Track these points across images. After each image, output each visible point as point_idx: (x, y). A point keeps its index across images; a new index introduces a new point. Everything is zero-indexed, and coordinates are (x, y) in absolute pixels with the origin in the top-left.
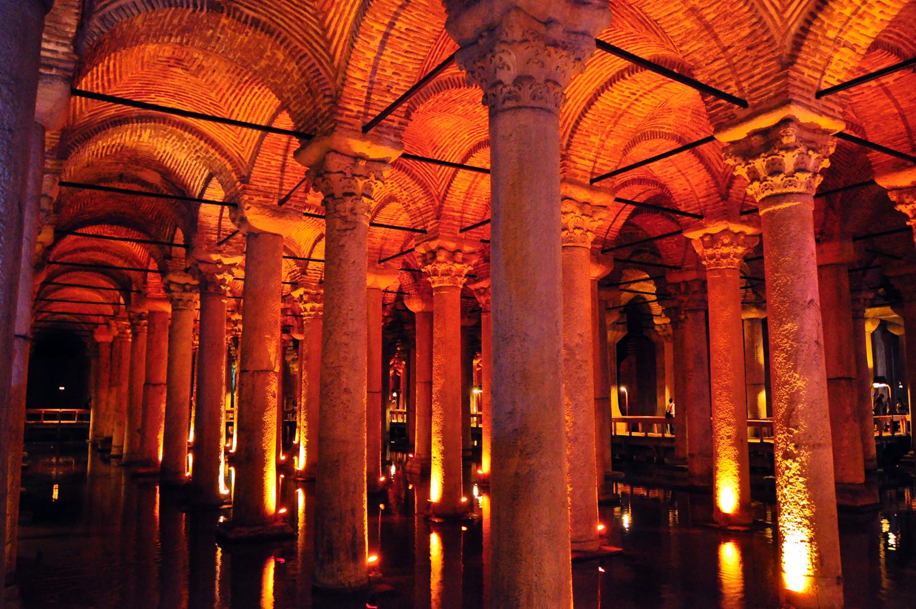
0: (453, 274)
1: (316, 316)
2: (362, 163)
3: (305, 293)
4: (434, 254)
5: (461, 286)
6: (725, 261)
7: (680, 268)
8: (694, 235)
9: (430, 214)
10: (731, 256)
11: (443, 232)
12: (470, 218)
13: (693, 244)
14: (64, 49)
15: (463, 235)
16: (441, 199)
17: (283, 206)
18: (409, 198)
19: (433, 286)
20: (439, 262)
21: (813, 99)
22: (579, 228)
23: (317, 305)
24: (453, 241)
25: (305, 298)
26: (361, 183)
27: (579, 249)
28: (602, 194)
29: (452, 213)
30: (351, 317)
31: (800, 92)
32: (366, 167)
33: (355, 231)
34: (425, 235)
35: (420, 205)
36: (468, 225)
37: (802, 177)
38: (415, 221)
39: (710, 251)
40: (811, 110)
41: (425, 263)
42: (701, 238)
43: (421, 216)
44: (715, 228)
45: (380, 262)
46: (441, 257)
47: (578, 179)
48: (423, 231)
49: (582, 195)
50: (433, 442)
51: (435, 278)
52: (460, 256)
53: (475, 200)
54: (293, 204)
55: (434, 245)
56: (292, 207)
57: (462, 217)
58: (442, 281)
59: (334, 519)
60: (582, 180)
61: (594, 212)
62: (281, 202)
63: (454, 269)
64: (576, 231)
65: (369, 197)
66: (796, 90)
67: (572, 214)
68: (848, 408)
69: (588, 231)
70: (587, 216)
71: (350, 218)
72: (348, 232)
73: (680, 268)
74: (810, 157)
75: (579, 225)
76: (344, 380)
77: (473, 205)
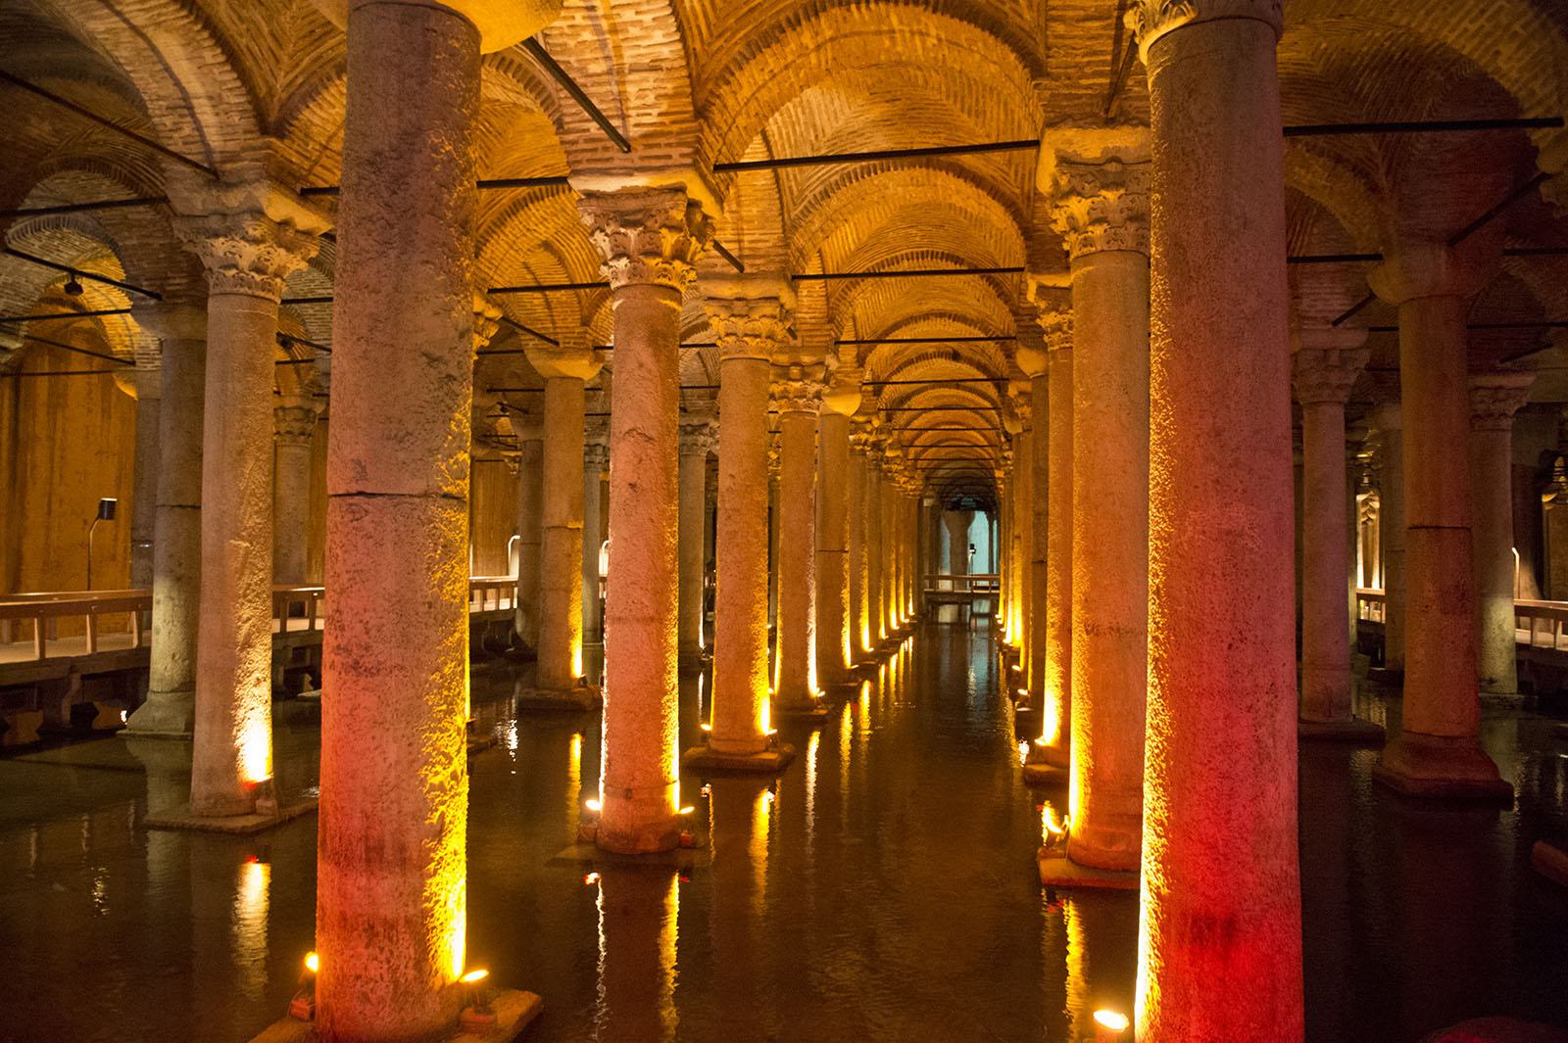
10: (1065, 328)
14: (184, 281)
21: (621, 155)
22: (727, 335)
28: (759, 282)
31: (588, 155)
37: (624, 261)
40: (612, 175)
47: (717, 270)
49: (727, 290)
52: (795, 371)
63: (788, 387)
67: (717, 319)
68: (1429, 586)
69: (746, 335)
74: (625, 235)
75: (730, 331)
77: (805, 299)
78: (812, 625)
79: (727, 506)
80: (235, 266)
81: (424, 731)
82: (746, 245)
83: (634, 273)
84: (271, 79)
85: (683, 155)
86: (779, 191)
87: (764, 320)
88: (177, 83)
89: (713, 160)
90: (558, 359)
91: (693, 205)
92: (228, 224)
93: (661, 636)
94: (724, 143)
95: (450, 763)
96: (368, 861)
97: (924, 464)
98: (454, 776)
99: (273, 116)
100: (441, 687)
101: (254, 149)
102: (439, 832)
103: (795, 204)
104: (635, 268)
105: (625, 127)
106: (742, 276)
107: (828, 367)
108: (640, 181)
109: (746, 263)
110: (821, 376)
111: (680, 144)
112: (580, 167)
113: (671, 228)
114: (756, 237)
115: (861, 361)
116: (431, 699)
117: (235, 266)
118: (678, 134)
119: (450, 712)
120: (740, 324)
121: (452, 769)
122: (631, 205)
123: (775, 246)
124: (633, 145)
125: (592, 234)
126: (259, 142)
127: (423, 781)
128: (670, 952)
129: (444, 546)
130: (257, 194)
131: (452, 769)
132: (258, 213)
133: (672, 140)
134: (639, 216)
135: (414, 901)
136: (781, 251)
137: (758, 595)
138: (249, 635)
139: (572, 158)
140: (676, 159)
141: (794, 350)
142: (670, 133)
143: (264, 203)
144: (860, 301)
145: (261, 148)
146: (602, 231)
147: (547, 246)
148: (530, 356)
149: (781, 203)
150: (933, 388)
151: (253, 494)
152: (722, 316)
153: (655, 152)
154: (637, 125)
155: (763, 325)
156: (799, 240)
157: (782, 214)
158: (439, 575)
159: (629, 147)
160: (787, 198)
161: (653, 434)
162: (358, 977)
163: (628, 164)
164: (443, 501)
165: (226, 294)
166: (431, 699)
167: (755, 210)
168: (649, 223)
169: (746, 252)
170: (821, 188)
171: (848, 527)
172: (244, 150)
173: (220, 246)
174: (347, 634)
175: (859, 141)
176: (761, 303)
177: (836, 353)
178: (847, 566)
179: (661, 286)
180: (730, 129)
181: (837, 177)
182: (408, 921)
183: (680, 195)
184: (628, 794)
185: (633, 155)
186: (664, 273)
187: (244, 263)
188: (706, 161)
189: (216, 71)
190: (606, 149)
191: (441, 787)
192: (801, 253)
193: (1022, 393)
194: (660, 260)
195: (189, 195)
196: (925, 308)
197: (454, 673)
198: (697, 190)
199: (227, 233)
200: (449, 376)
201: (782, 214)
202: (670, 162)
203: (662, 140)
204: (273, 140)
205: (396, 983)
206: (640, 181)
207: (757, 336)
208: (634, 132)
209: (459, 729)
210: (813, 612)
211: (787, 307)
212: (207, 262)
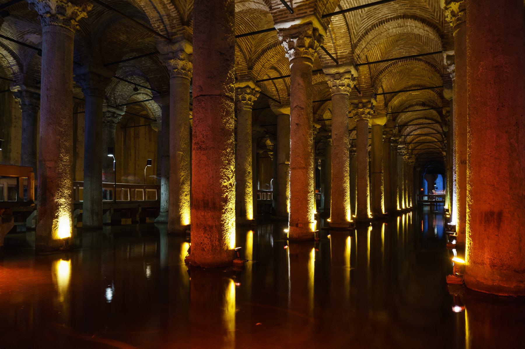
2: (239, 90)
21: (290, 15)
22: (333, 86)
26: (240, 97)
31: (280, 17)
32: (241, 91)
37: (292, 51)
47: (329, 64)
49: (333, 71)
52: (360, 105)
60: (332, 64)
61: (341, 77)
65: (244, 100)
66: (277, 17)
69: (340, 86)
74: (293, 41)
78: (368, 193)
79: (335, 144)
80: (177, 68)
81: (221, 168)
82: (339, 54)
83: (296, 54)
84: (184, 7)
85: (311, 11)
86: (349, 33)
87: (346, 80)
88: (158, 12)
89: (321, 14)
91: (315, 30)
92: (175, 55)
93: (307, 173)
94: (325, 8)
95: (229, 180)
96: (204, 207)
97: (415, 152)
98: (230, 184)
99: (186, 19)
100: (226, 155)
101: (180, 30)
102: (226, 201)
103: (355, 38)
104: (296, 52)
105: (291, 4)
106: (338, 66)
107: (372, 104)
108: (297, 22)
109: (339, 60)
110: (370, 106)
111: (309, 8)
112: (278, 21)
113: (308, 37)
114: (342, 51)
115: (386, 105)
116: (223, 158)
117: (177, 68)
118: (309, 4)
119: (229, 164)
120: (338, 82)
121: (230, 182)
122: (294, 31)
123: (349, 53)
124: (294, 10)
125: (282, 43)
126: (181, 28)
127: (221, 184)
128: (289, 210)
129: (226, 112)
130: (182, 45)
131: (230, 182)
132: (182, 50)
133: (307, 7)
134: (297, 35)
135: (218, 221)
136: (351, 55)
137: (346, 174)
138: (183, 180)
139: (275, 18)
140: (309, 13)
141: (360, 98)
142: (306, 4)
143: (184, 47)
144: (384, 80)
145: (182, 30)
146: (285, 41)
147: (273, 68)
148: (272, 108)
149: (350, 38)
150: (416, 119)
151: (184, 138)
152: (332, 80)
153: (302, 12)
154: (295, 3)
155: (346, 82)
156: (357, 51)
157: (351, 42)
158: (225, 120)
159: (293, 11)
160: (353, 36)
161: (303, 106)
162: (201, 243)
163: (293, 17)
164: (225, 98)
165: (174, 77)
166: (223, 158)
167: (341, 41)
168: (300, 36)
169: (339, 57)
170: (364, 31)
171: (383, 164)
172: (178, 31)
173: (172, 62)
174: (198, 138)
175: (377, 12)
177: (375, 98)
178: (382, 178)
179: (305, 57)
180: (327, 3)
181: (370, 27)
182: (216, 226)
183: (310, 25)
184: (297, 225)
185: (295, 14)
186: (306, 53)
187: (179, 67)
188: (319, 13)
189: (168, 6)
190: (286, 13)
191: (226, 186)
192: (359, 57)
194: (304, 48)
195: (164, 48)
196: (410, 84)
197: (230, 152)
198: (316, 24)
199: (174, 58)
200: (227, 60)
201: (351, 42)
202: (306, 14)
203: (304, 7)
204: (185, 27)
205: (213, 246)
206: (297, 22)
207: (344, 86)
208: (294, 6)
209: (232, 171)
210: (368, 188)
211: (354, 76)
212: (169, 68)
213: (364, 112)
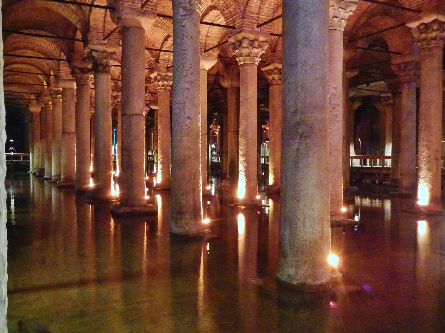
0: (252, 55)
1: (165, 89)
3: (158, 75)
4: (240, 42)
5: (257, 64)
6: (433, 42)
7: (400, 54)
8: (413, 25)
9: (237, 15)
11: (246, 27)
12: (264, 18)
13: (413, 32)
15: (259, 30)
16: (244, 5)
17: (144, 9)
18: (224, 5)
19: (240, 64)
20: (243, 48)
22: (336, 17)
23: (166, 83)
24: (252, 34)
25: (158, 78)
27: (336, 31)
29: (251, 15)
30: (191, 72)
33: (192, 16)
34: (234, 30)
35: (231, 9)
36: (262, 23)
38: (228, 21)
39: (423, 36)
41: (235, 48)
42: (418, 27)
43: (232, 17)
44: (427, 20)
45: (205, 51)
46: (245, 43)
48: (234, 28)
50: (240, 161)
51: (241, 58)
52: (257, 43)
53: (267, 6)
54: (150, 7)
55: (240, 36)
56: (150, 10)
57: (258, 17)
58: (245, 61)
59: (183, 194)
61: (347, 6)
62: (142, 6)
63: (252, 51)
64: (335, 19)
67: (332, 8)
69: (342, 19)
70: (342, 8)
71: (189, 7)
72: (188, 17)
73: (400, 54)
75: (336, 15)
76: (187, 111)
77: (265, 9)
90: (143, 16)
176: (352, 4)
193: (276, 68)
213: (258, 54)
